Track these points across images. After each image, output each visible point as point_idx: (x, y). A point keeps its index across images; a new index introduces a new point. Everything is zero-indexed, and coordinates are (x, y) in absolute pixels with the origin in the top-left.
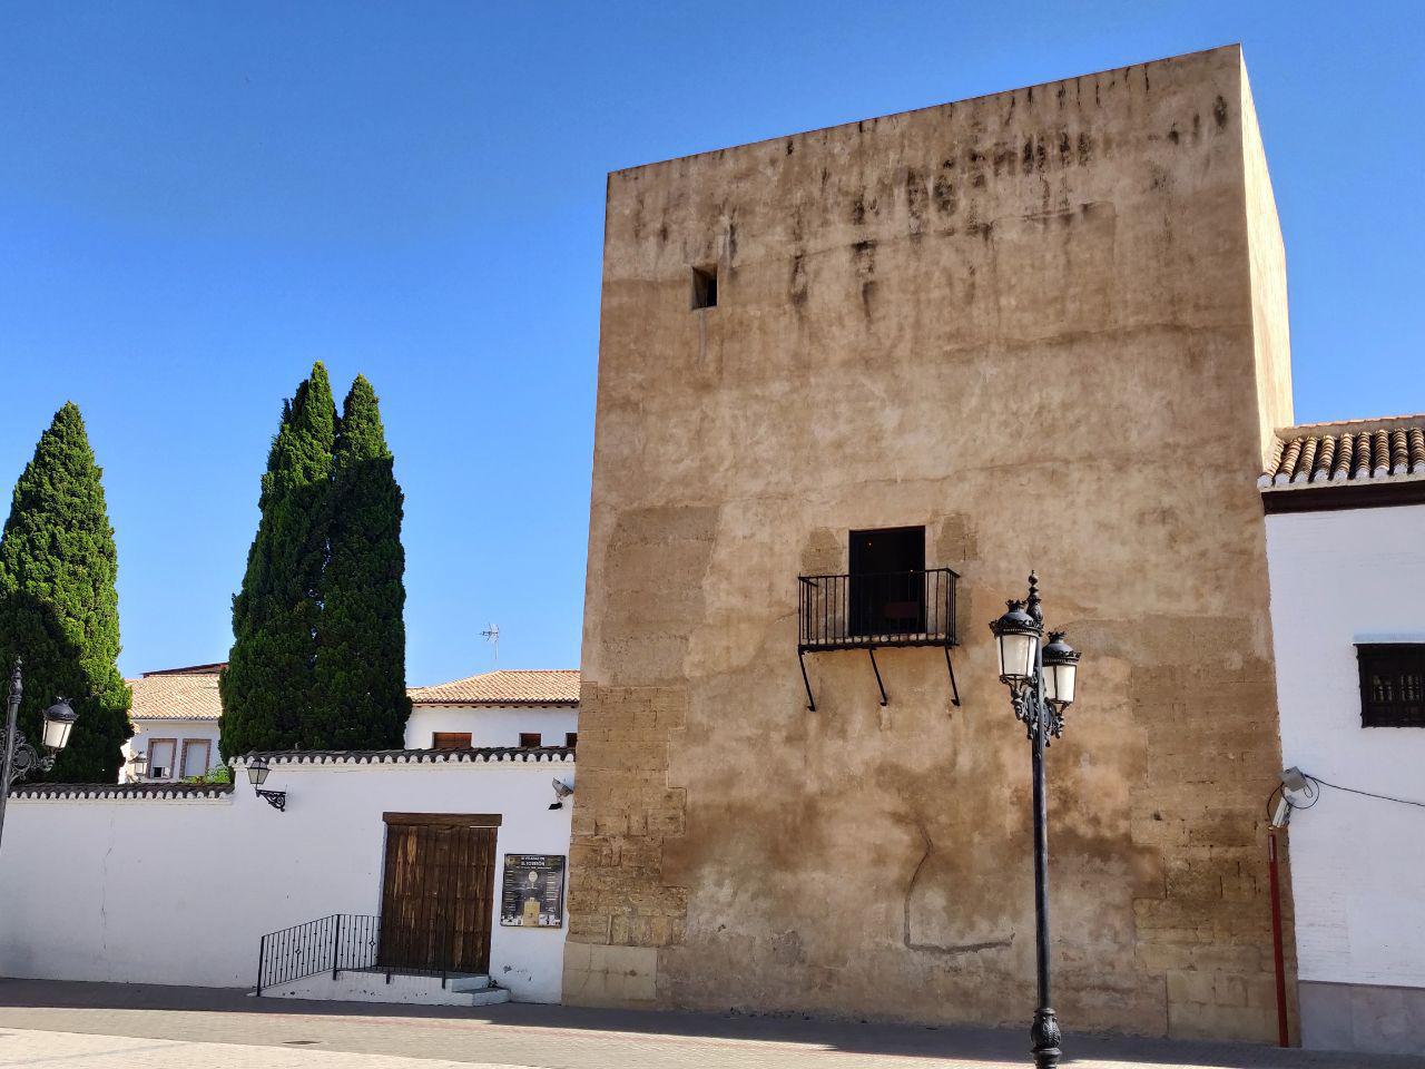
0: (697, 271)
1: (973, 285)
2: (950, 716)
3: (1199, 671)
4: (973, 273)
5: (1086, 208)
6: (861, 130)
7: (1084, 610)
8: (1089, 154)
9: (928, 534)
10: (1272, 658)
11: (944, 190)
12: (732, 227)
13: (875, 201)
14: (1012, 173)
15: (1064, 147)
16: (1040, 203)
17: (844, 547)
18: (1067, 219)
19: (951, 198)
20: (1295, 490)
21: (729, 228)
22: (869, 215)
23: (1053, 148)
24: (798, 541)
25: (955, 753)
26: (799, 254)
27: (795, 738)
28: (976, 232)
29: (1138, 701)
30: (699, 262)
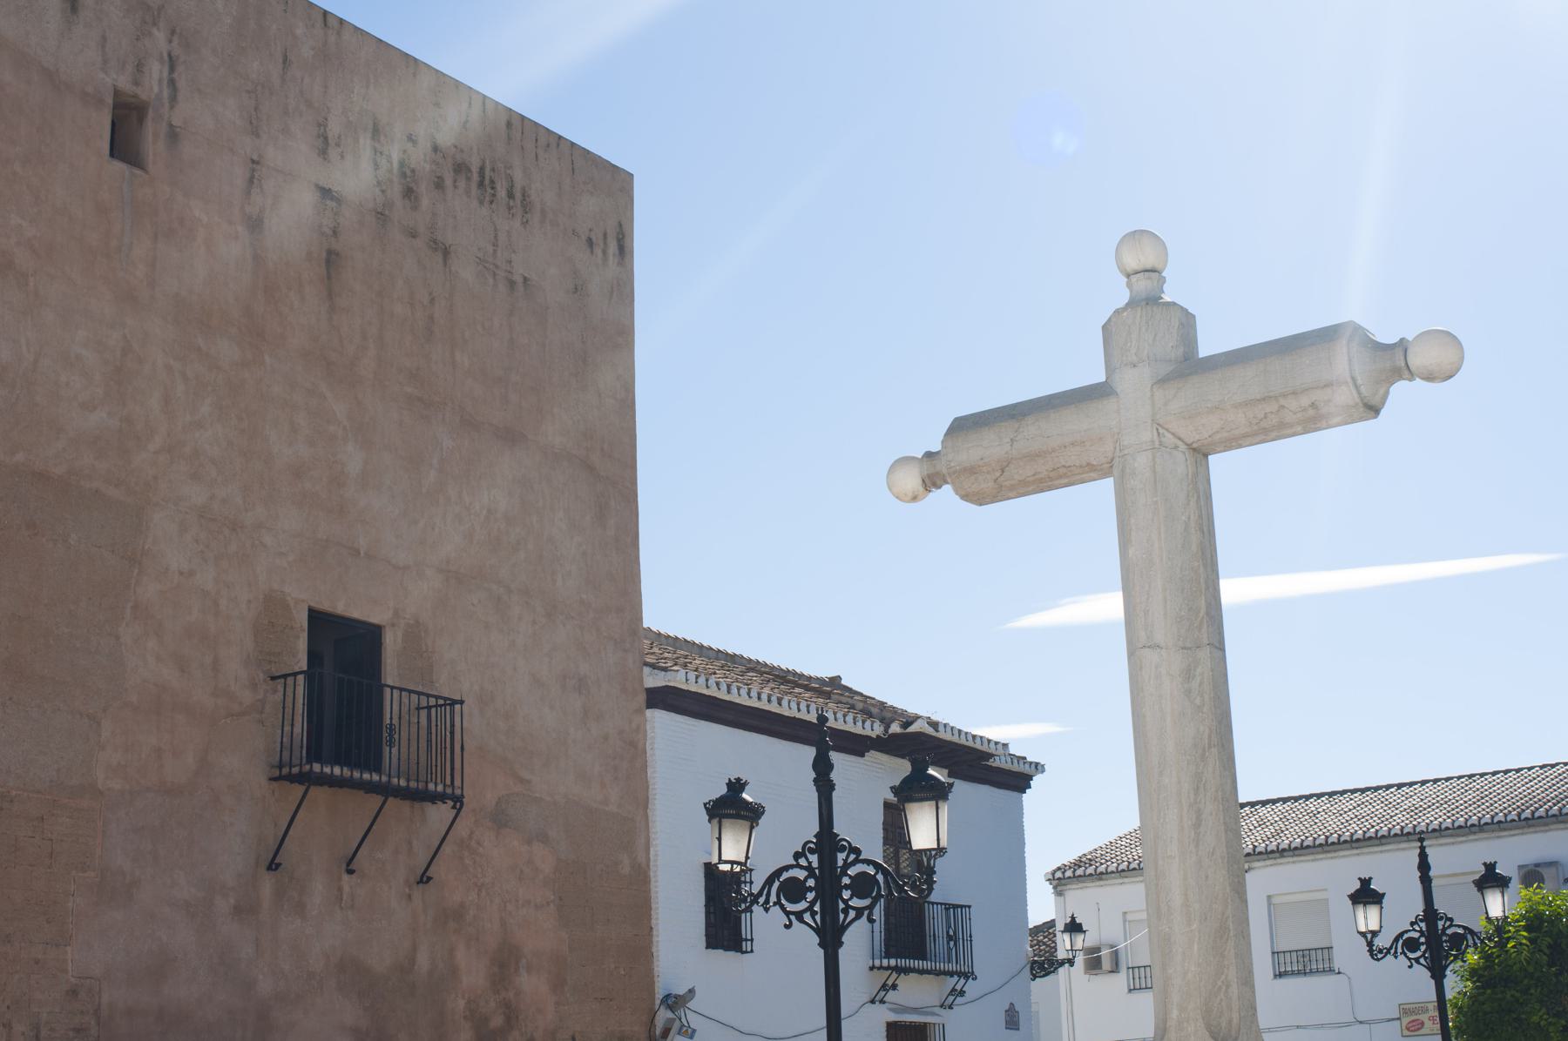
0: (117, 93)
1: (431, 318)
2: (410, 897)
3: (602, 870)
4: (432, 301)
5: (525, 279)
6: (325, 25)
7: (522, 781)
8: (529, 216)
9: (391, 642)
10: (648, 866)
11: (408, 173)
12: (170, 55)
13: (339, 137)
14: (468, 192)
15: (511, 195)
16: (490, 249)
17: (304, 630)
18: (512, 284)
19: (415, 188)
20: (688, 691)
21: (165, 55)
22: (333, 153)
23: (502, 188)
24: (249, 601)
25: (414, 948)
26: (255, 157)
27: (245, 910)
28: (436, 250)
29: (561, 899)
30: (124, 82)
